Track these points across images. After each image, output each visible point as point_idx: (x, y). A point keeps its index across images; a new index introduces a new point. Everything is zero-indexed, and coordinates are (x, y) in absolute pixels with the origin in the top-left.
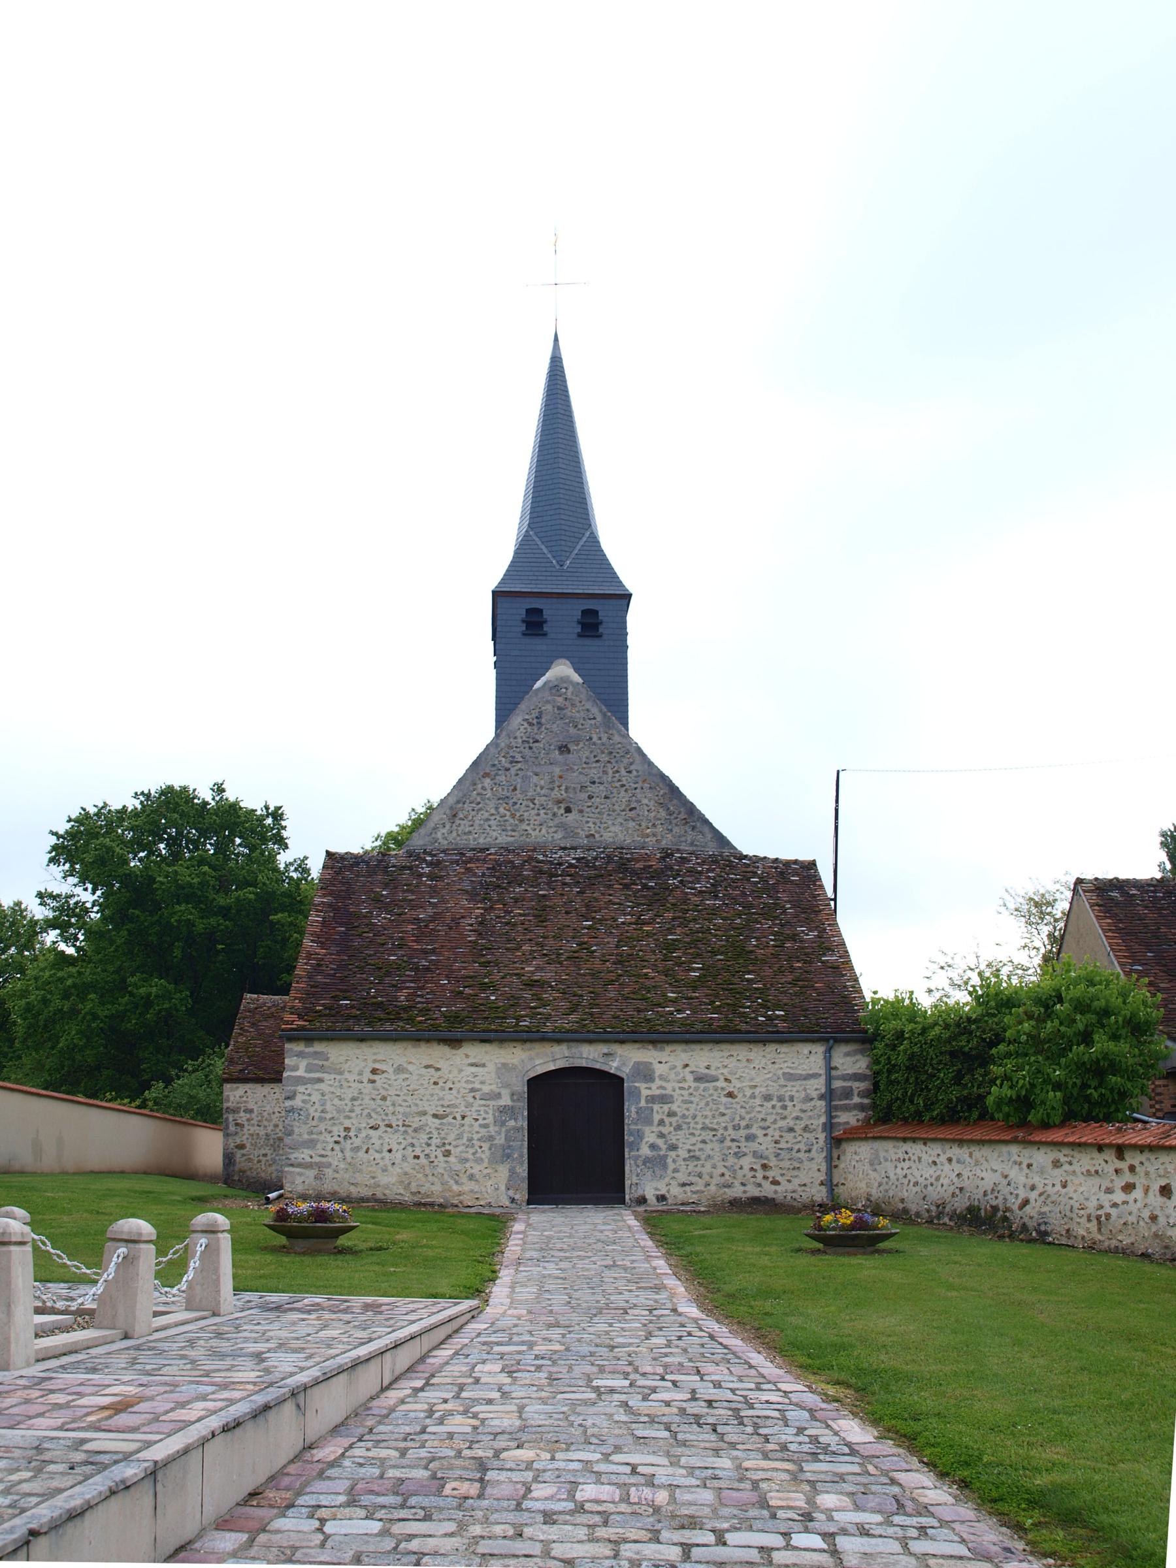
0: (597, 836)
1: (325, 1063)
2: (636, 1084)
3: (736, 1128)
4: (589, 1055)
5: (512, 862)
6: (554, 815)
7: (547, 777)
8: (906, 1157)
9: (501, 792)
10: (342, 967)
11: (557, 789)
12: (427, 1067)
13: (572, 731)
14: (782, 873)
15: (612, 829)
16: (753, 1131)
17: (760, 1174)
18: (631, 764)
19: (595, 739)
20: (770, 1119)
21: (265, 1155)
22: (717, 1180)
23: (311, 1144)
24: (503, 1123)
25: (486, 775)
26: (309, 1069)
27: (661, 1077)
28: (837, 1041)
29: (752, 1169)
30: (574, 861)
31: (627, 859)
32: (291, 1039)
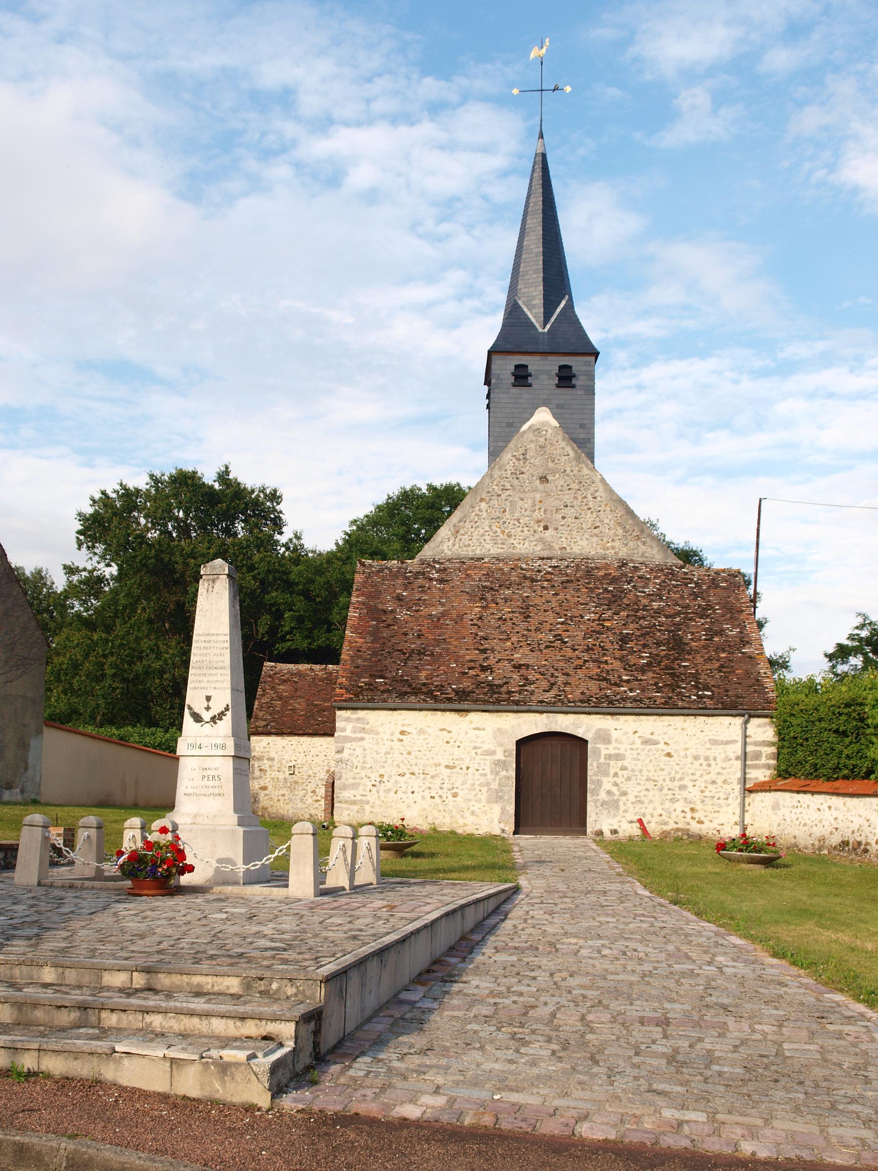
0: (568, 548)
1: (366, 726)
2: (598, 746)
3: (672, 780)
4: (563, 723)
5: (501, 569)
7: (530, 502)
8: (799, 805)
10: (374, 654)
11: (537, 511)
12: (442, 730)
13: (551, 465)
14: (713, 580)
15: (580, 543)
16: (684, 782)
17: (689, 815)
18: (596, 491)
20: (698, 774)
21: (283, 795)
22: (657, 819)
23: (355, 786)
24: (497, 773)
25: (482, 500)
28: (751, 716)
29: (683, 811)
30: (550, 569)
31: (592, 568)
32: (340, 709)
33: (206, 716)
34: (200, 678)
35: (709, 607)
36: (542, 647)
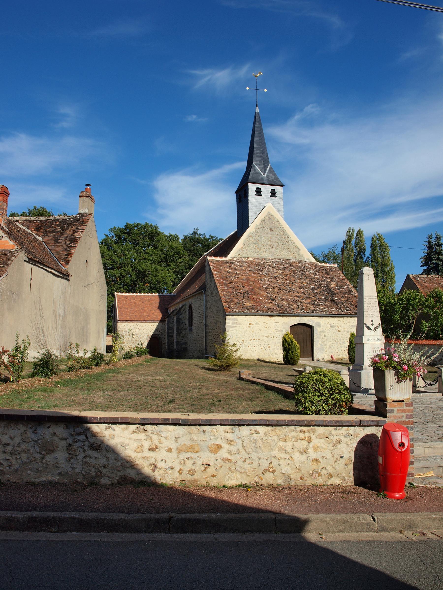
6: (269, 249)
9: (255, 242)
19: (279, 227)
26: (232, 324)
27: (323, 326)
32: (227, 315)
33: (372, 328)
34: (368, 313)
35: (333, 278)
36: (287, 292)
